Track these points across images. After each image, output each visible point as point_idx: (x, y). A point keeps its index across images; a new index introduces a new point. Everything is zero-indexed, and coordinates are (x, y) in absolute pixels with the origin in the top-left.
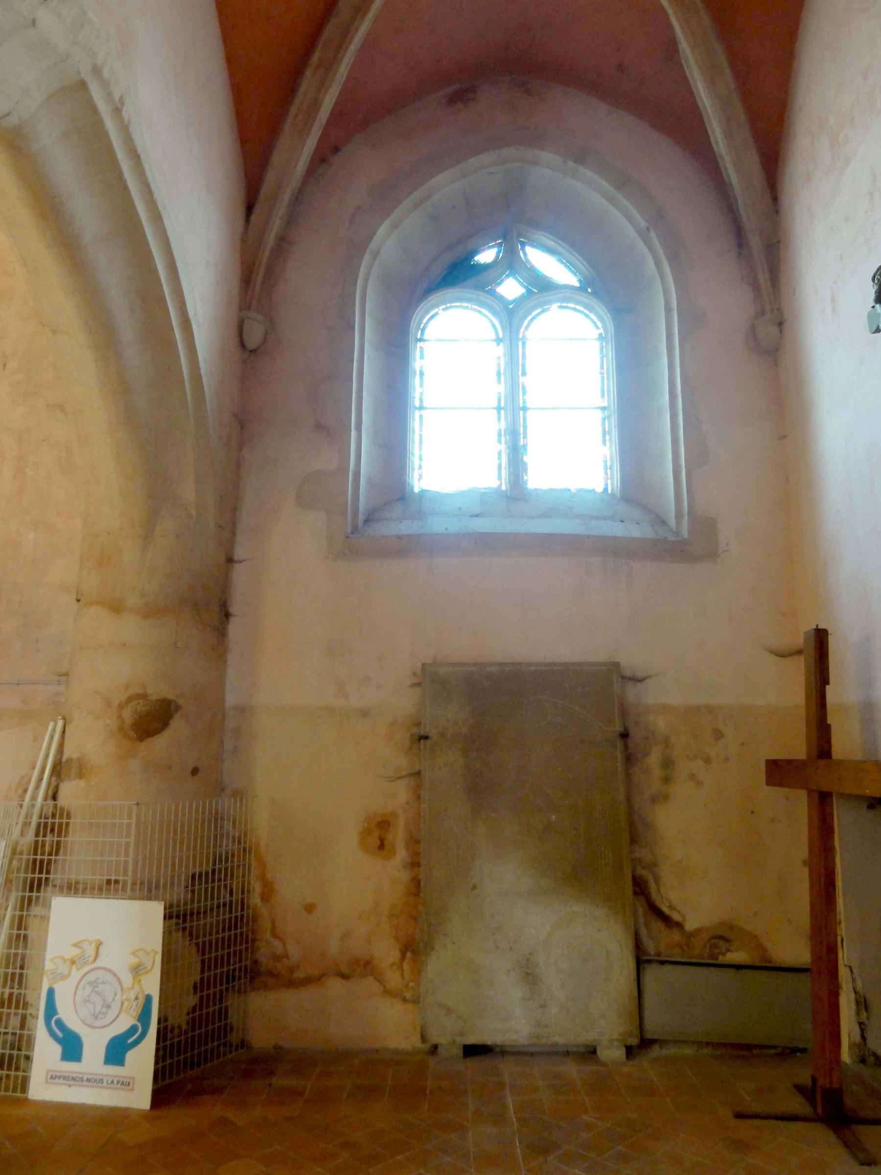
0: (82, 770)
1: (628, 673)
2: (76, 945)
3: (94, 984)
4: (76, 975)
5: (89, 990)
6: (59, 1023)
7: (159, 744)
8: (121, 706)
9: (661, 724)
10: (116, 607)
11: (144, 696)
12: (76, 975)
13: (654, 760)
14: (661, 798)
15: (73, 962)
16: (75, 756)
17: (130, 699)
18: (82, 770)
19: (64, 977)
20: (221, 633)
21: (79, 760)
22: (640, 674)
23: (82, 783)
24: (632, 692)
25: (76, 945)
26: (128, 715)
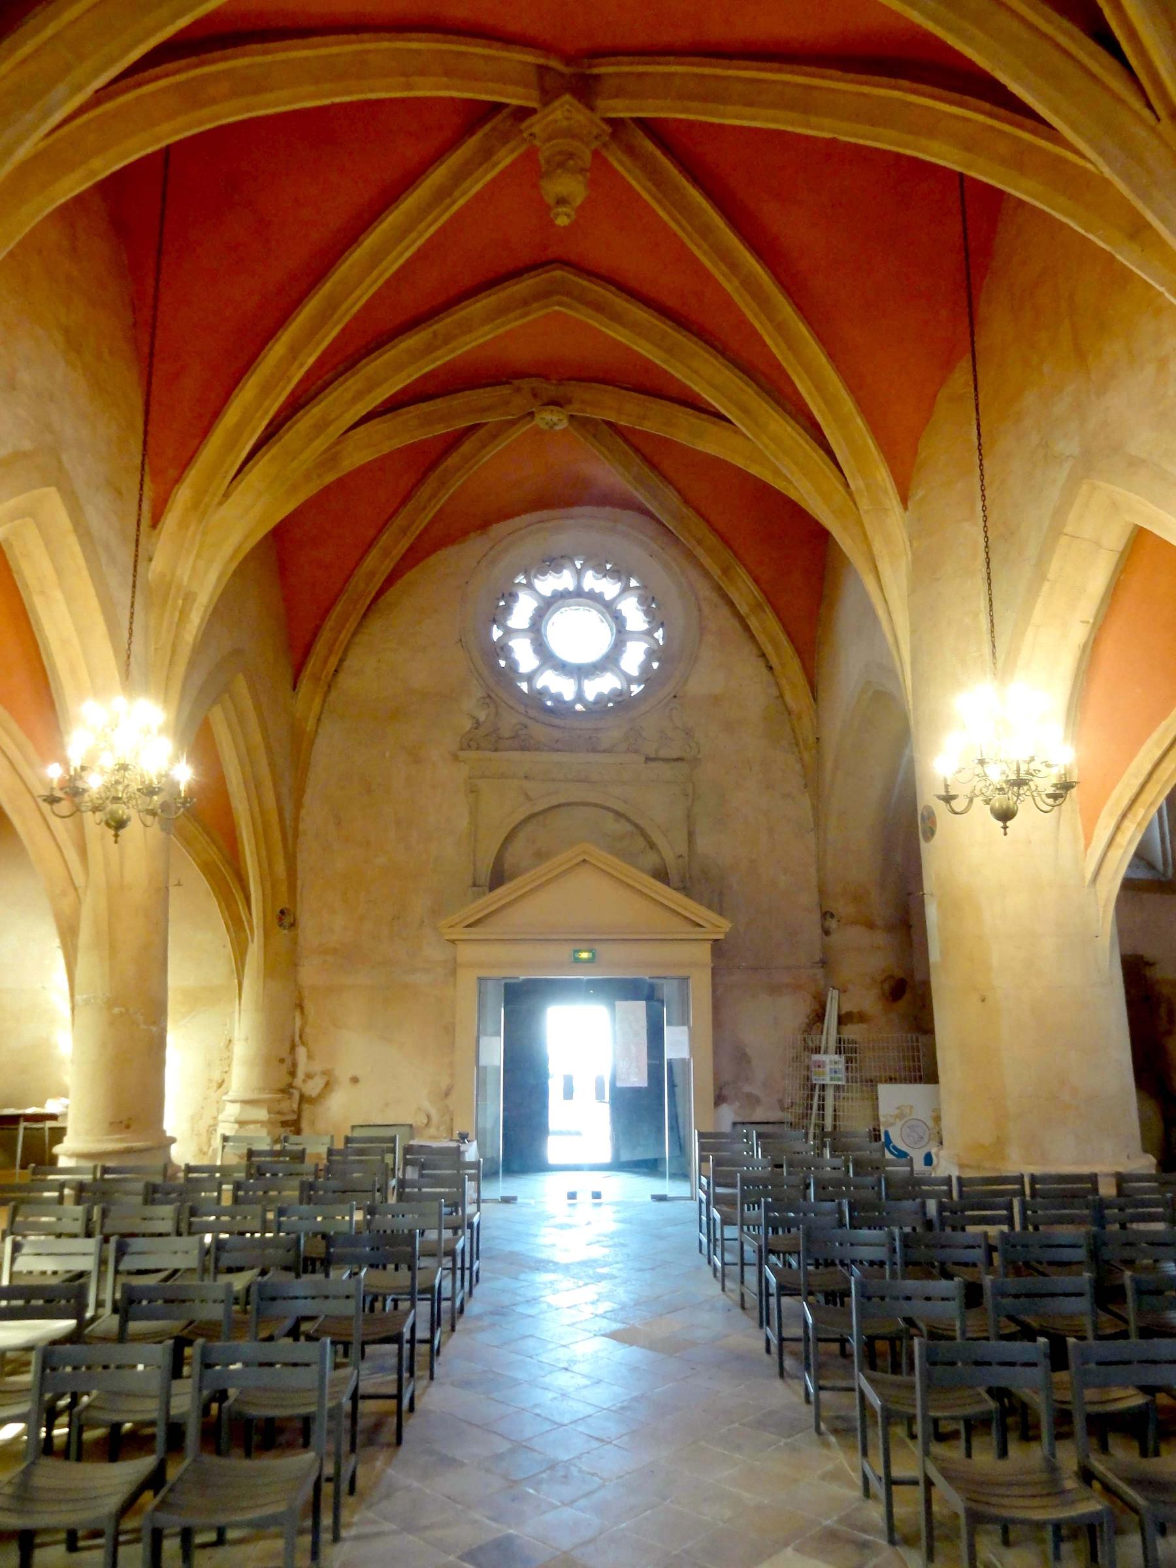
0: (861, 1018)
1: (1146, 960)
2: (897, 1108)
3: (911, 1127)
4: (899, 1123)
5: (908, 1130)
6: (894, 1147)
7: (902, 1004)
8: (883, 982)
9: (1166, 990)
10: (871, 926)
11: (891, 977)
12: (899, 1123)
13: (1163, 1011)
14: (1169, 1033)
15: (897, 1117)
16: (855, 1011)
17: (885, 980)
18: (861, 1018)
19: (892, 1124)
20: (909, 935)
21: (858, 1012)
22: (1151, 961)
23: (864, 1026)
24: (1149, 972)
25: (897, 1108)
26: (886, 986)
